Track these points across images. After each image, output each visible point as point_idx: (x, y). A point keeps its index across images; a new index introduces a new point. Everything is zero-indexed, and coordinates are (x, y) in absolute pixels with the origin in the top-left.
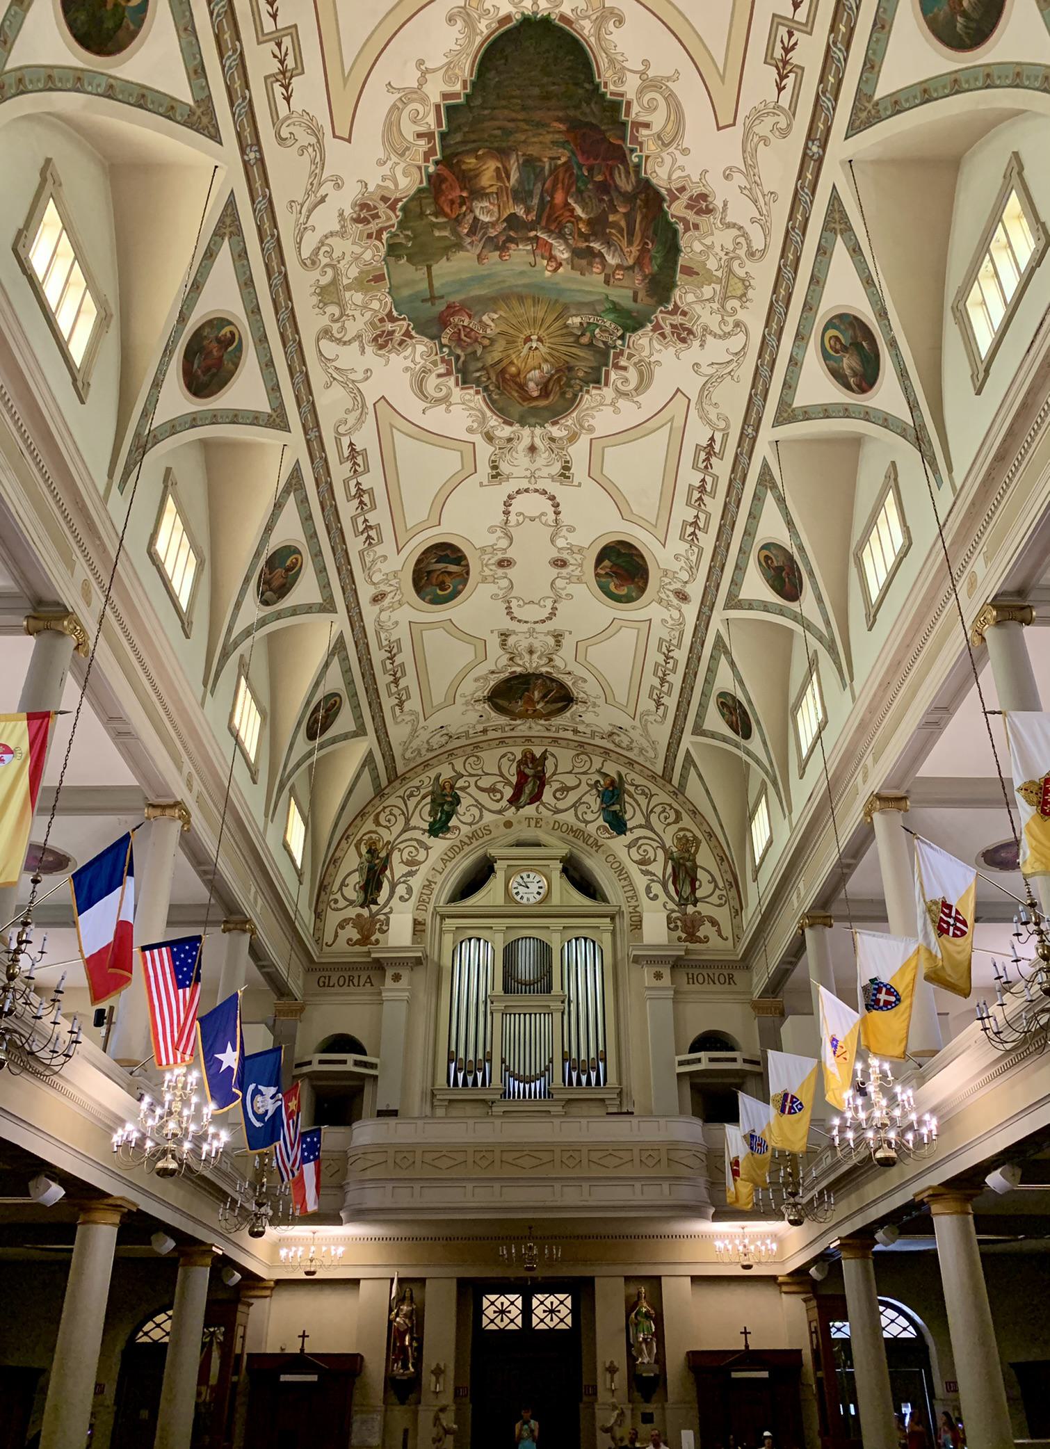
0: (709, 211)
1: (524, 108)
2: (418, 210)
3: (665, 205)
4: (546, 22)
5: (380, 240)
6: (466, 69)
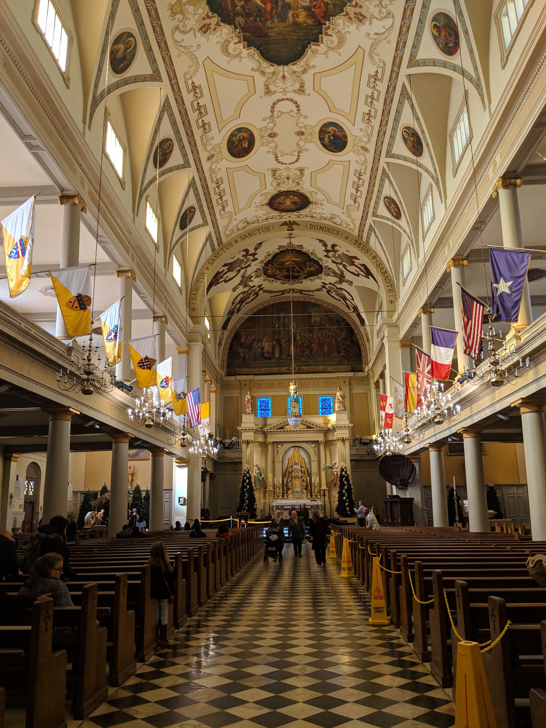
0: (201, 29)
1: (287, 39)
2: (336, 8)
3: (220, 19)
4: (279, 64)
5: (356, 2)
6: (309, 52)
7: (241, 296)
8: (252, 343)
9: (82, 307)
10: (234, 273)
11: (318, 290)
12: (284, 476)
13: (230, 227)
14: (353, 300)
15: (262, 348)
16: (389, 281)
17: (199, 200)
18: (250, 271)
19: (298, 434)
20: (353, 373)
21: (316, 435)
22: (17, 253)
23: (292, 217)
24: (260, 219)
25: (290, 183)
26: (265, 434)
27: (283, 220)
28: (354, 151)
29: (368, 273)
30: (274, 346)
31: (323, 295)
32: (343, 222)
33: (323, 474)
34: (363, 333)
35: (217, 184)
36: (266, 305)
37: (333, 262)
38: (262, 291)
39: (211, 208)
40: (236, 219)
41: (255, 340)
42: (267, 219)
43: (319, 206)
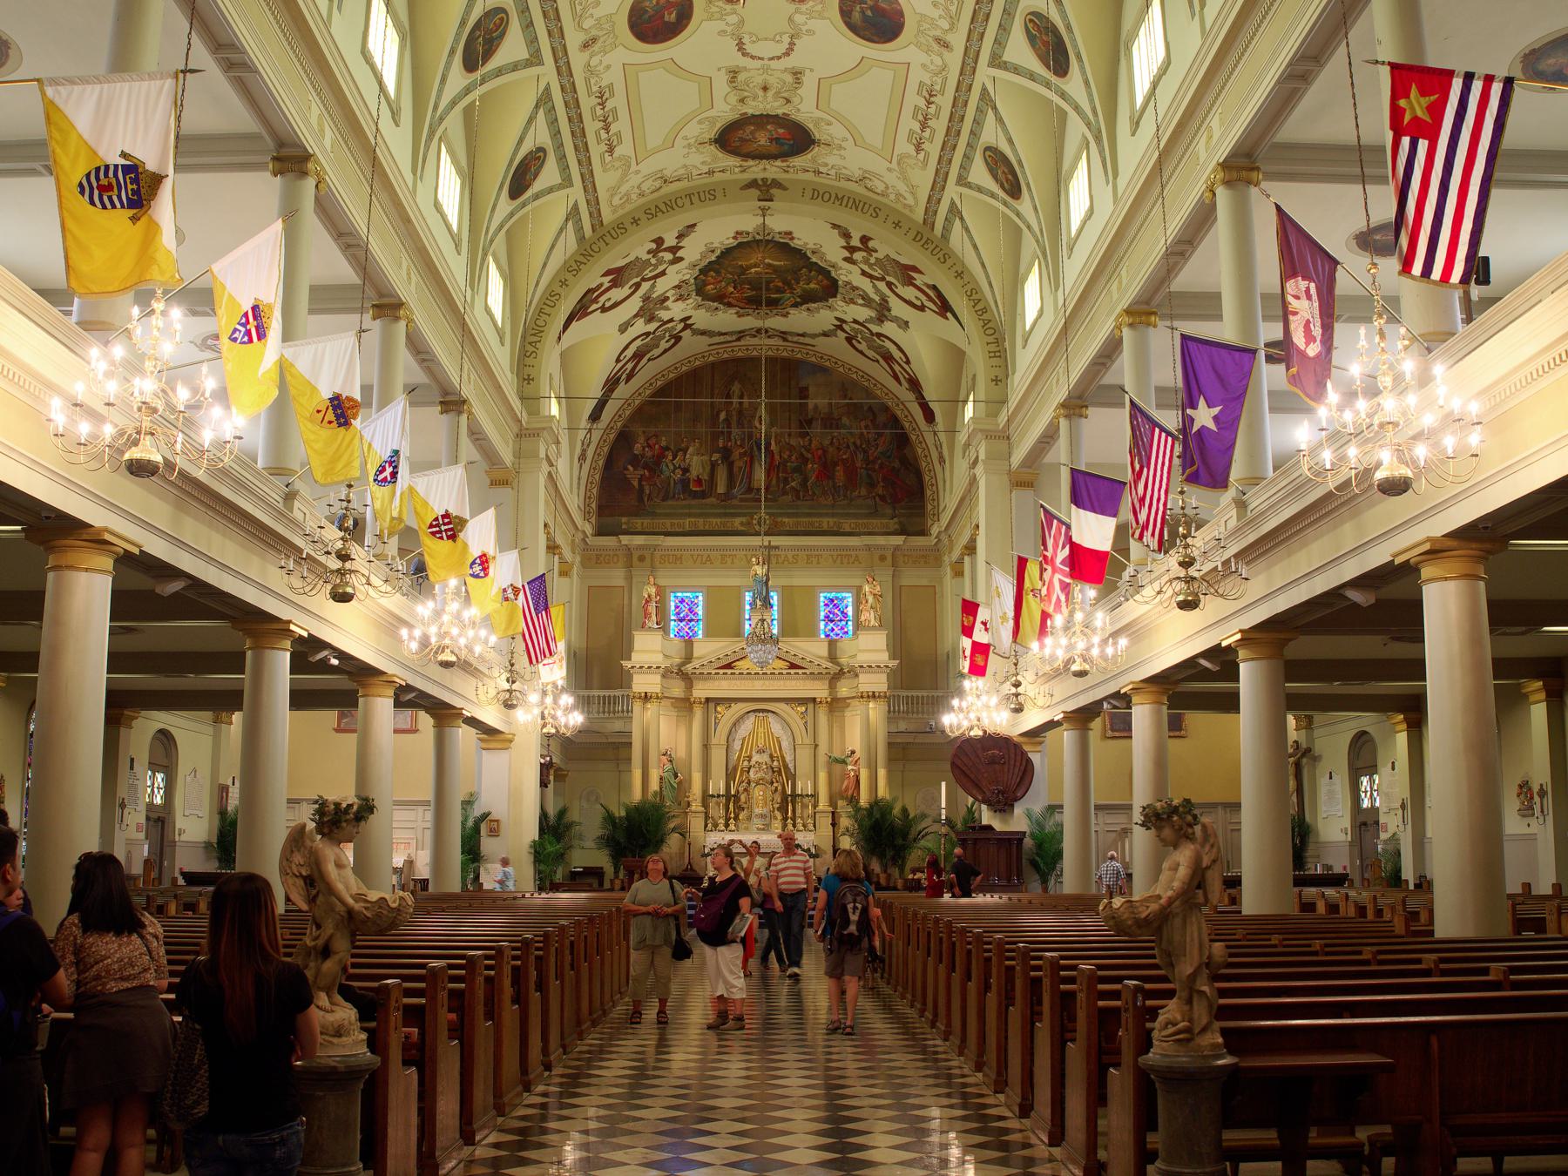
7: (638, 343)
8: (661, 456)
9: (342, 420)
10: (626, 291)
11: (825, 334)
12: (730, 776)
13: (623, 189)
14: (908, 362)
15: (686, 470)
16: (992, 331)
17: (556, 134)
18: (663, 286)
19: (767, 682)
20: (903, 537)
22: (248, 333)
23: (771, 170)
24: (695, 172)
25: (770, 99)
26: (688, 679)
27: (748, 176)
28: (918, 45)
29: (945, 308)
30: (713, 466)
31: (837, 347)
32: (890, 190)
33: (822, 776)
34: (929, 438)
35: (601, 97)
36: (698, 363)
37: (864, 273)
38: (688, 332)
39: (582, 149)
40: (637, 172)
41: (668, 449)
42: (711, 172)
43: (835, 152)
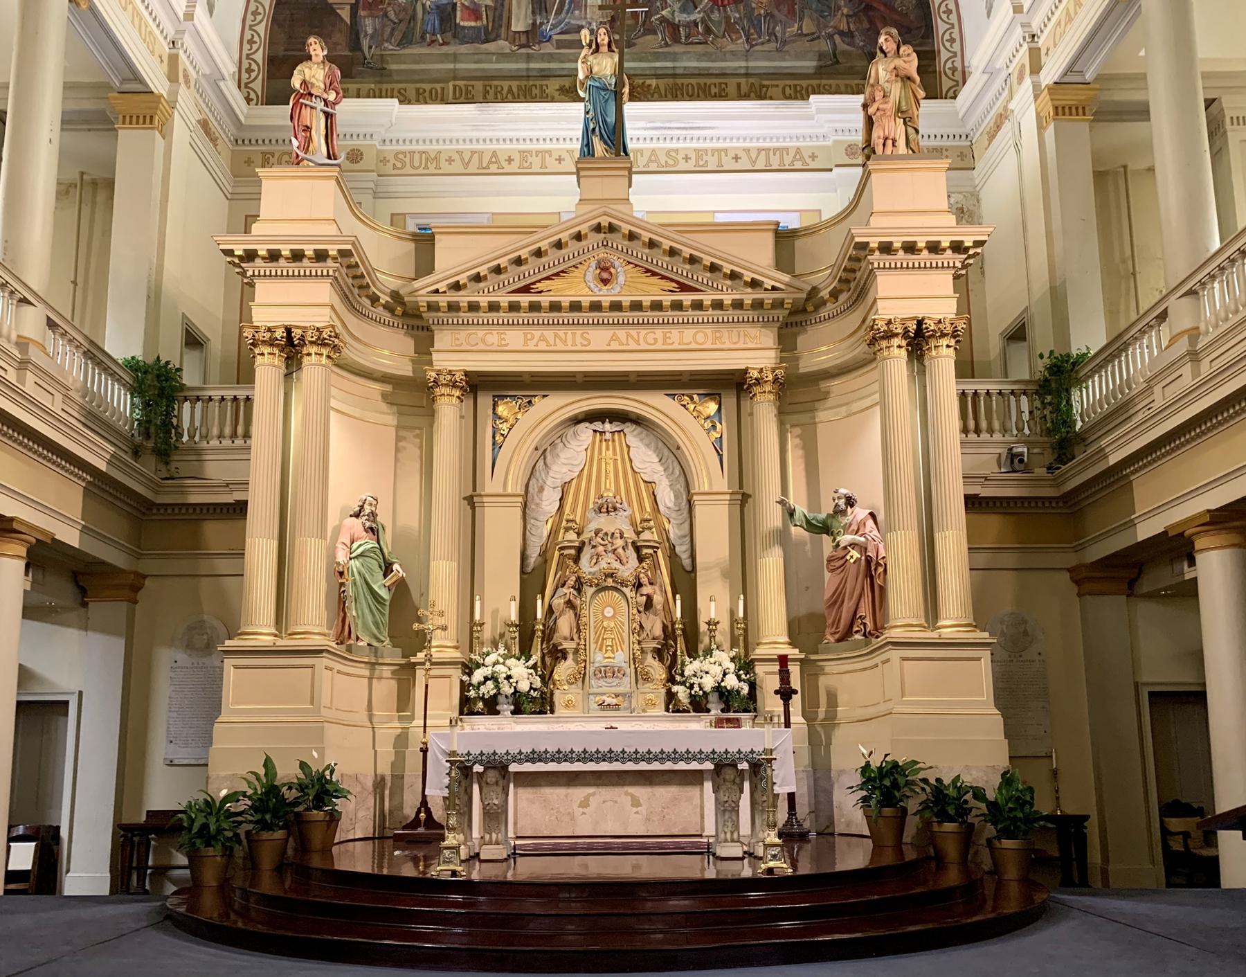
21: (728, 337)
